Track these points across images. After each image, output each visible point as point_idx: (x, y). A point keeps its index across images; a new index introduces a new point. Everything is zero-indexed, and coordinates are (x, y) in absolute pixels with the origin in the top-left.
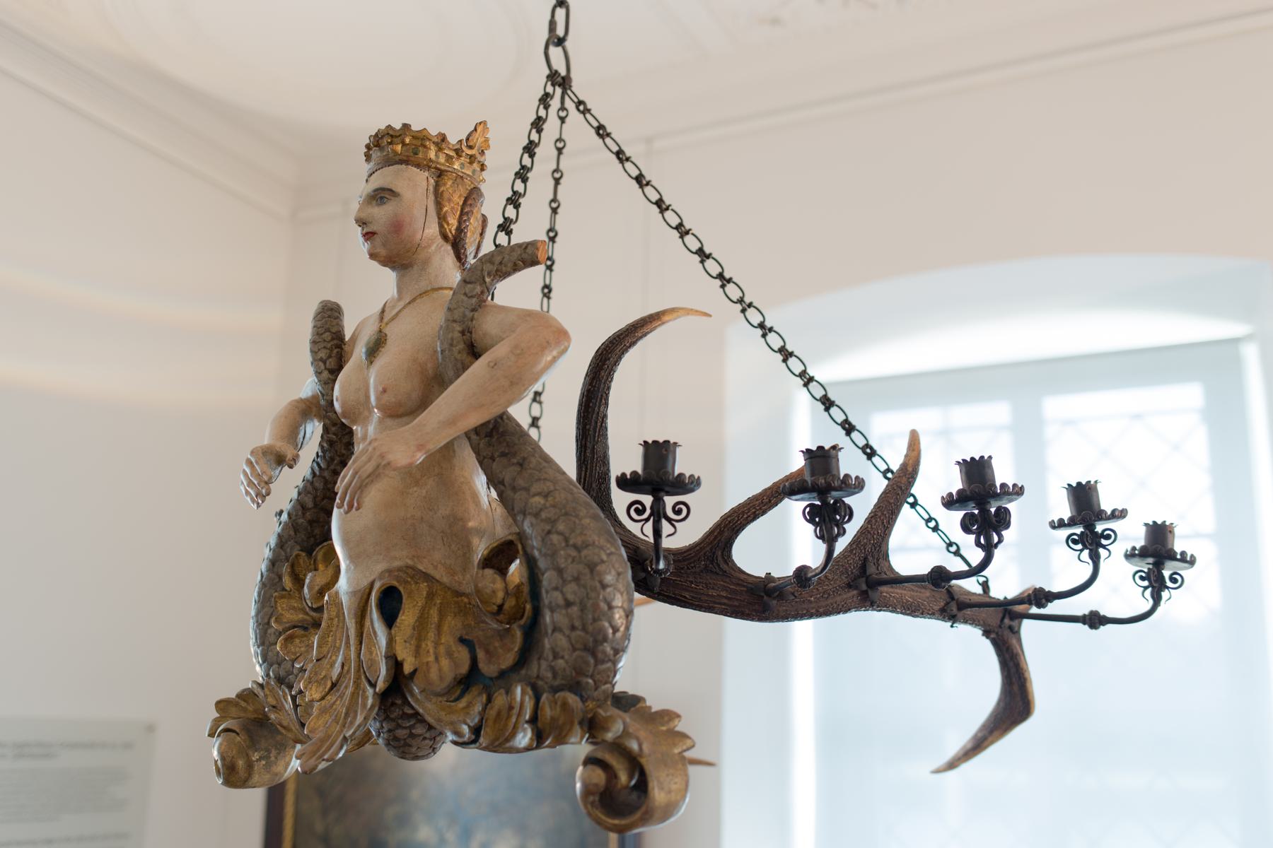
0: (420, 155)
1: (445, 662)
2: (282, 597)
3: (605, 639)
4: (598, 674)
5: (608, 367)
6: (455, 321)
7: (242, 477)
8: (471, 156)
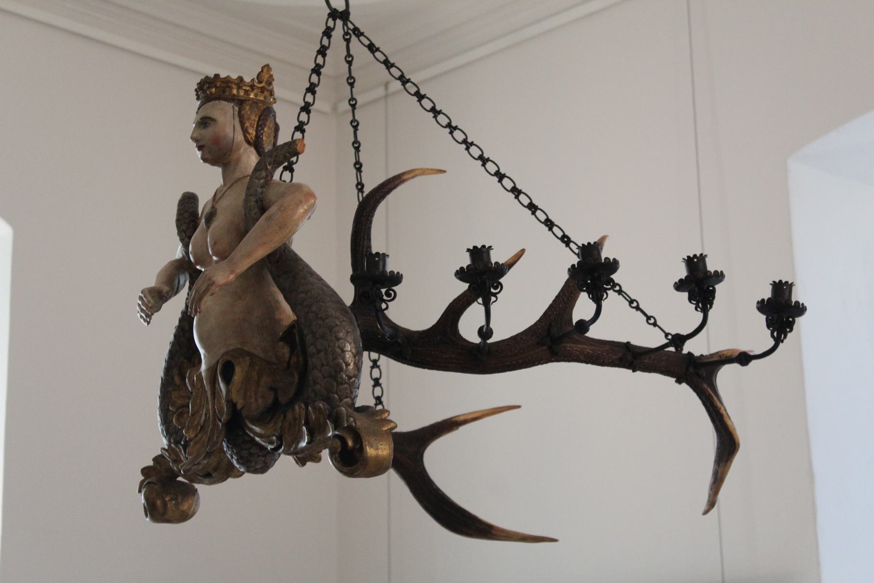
0: (227, 93)
1: (260, 401)
2: (174, 390)
3: (341, 370)
4: (340, 391)
5: (366, 214)
6: (251, 195)
7: (138, 308)
8: (262, 88)
